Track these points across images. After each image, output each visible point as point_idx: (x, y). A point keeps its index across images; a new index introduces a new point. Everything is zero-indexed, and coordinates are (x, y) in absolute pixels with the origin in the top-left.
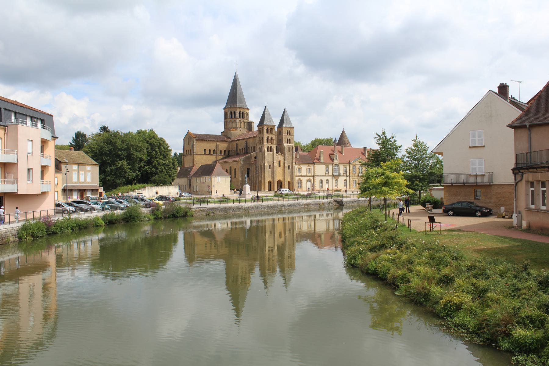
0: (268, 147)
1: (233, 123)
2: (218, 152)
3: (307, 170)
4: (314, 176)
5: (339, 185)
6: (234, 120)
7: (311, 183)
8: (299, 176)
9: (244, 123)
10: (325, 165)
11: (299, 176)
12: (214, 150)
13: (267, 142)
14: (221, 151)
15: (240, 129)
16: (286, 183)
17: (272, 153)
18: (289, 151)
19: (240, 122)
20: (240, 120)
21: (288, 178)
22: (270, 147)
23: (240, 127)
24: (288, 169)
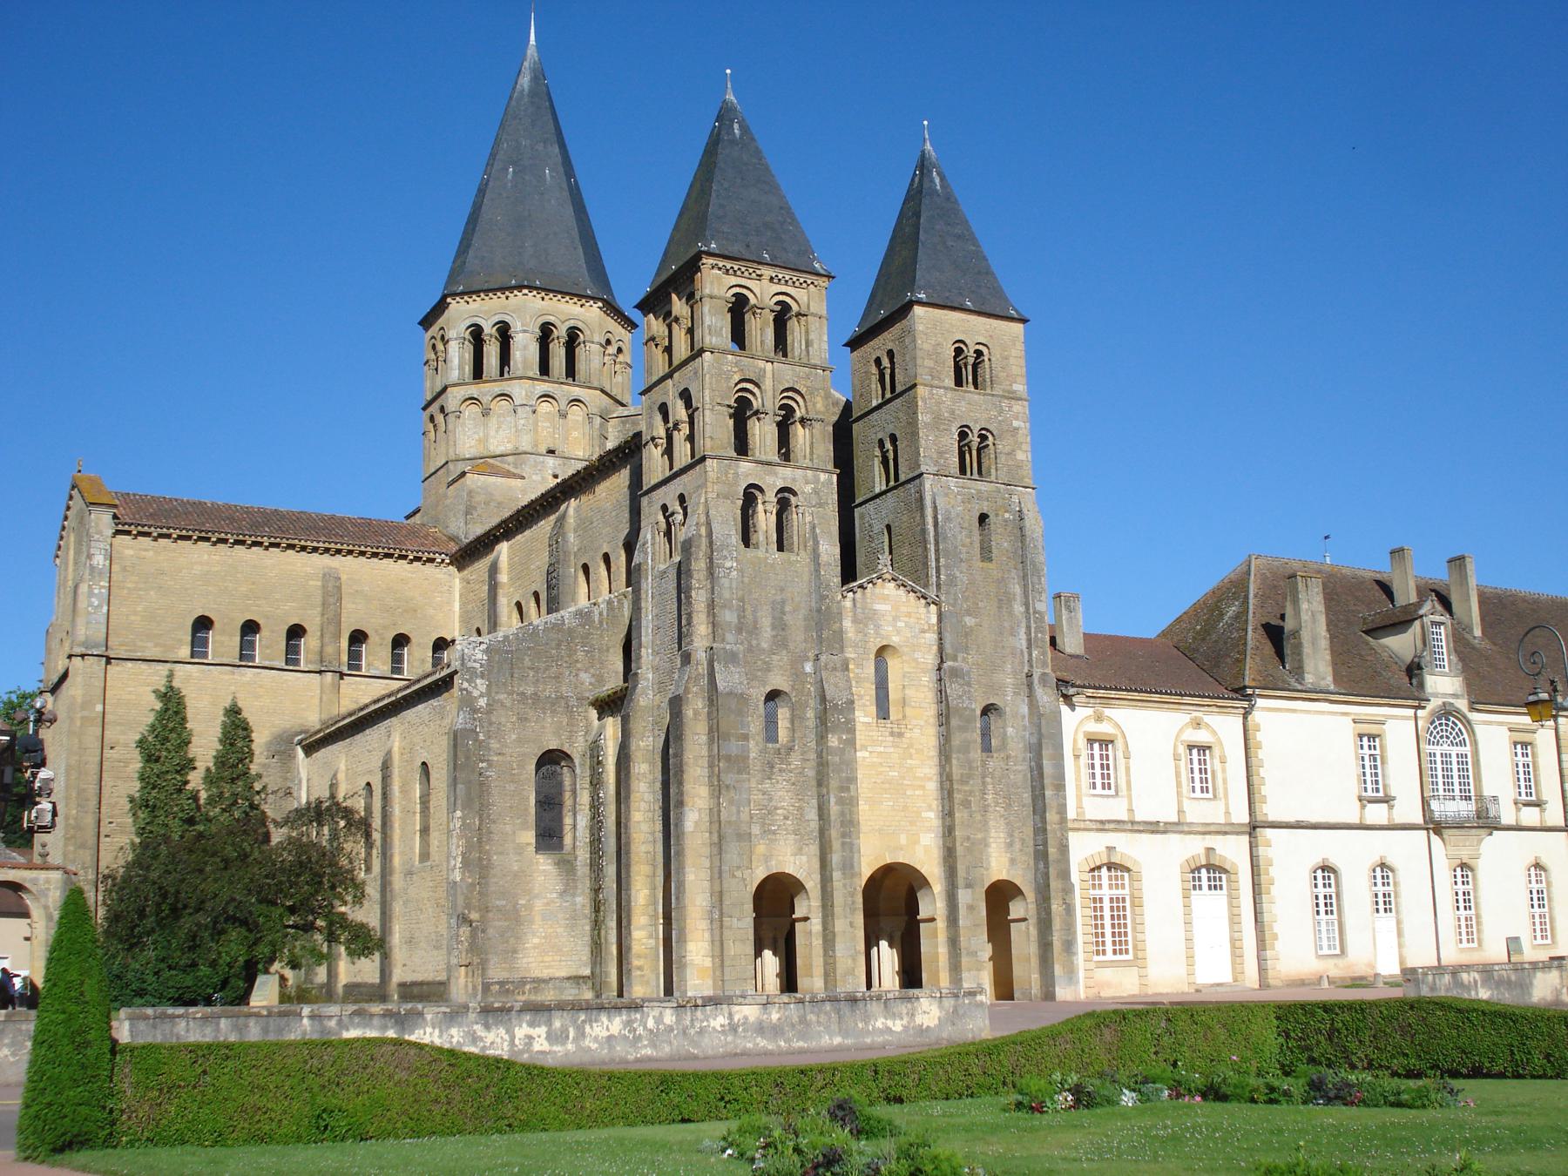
0: (750, 497)
1: (493, 421)
2: (329, 649)
3: (1177, 758)
4: (1253, 828)
5: (1485, 918)
6: (497, 388)
7: (1233, 899)
8: (1103, 826)
9: (589, 417)
10: (1349, 720)
11: (1103, 826)
12: (296, 632)
13: (742, 446)
14: (358, 637)
15: (550, 461)
16: (964, 897)
17: (799, 559)
18: (986, 553)
19: (545, 407)
20: (543, 387)
21: (985, 843)
22: (771, 496)
23: (551, 452)
24: (987, 748)
